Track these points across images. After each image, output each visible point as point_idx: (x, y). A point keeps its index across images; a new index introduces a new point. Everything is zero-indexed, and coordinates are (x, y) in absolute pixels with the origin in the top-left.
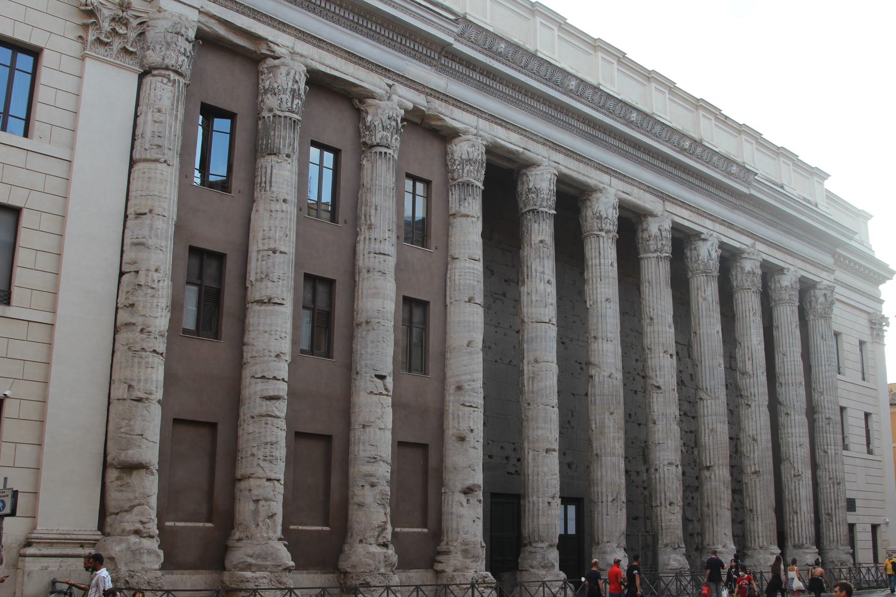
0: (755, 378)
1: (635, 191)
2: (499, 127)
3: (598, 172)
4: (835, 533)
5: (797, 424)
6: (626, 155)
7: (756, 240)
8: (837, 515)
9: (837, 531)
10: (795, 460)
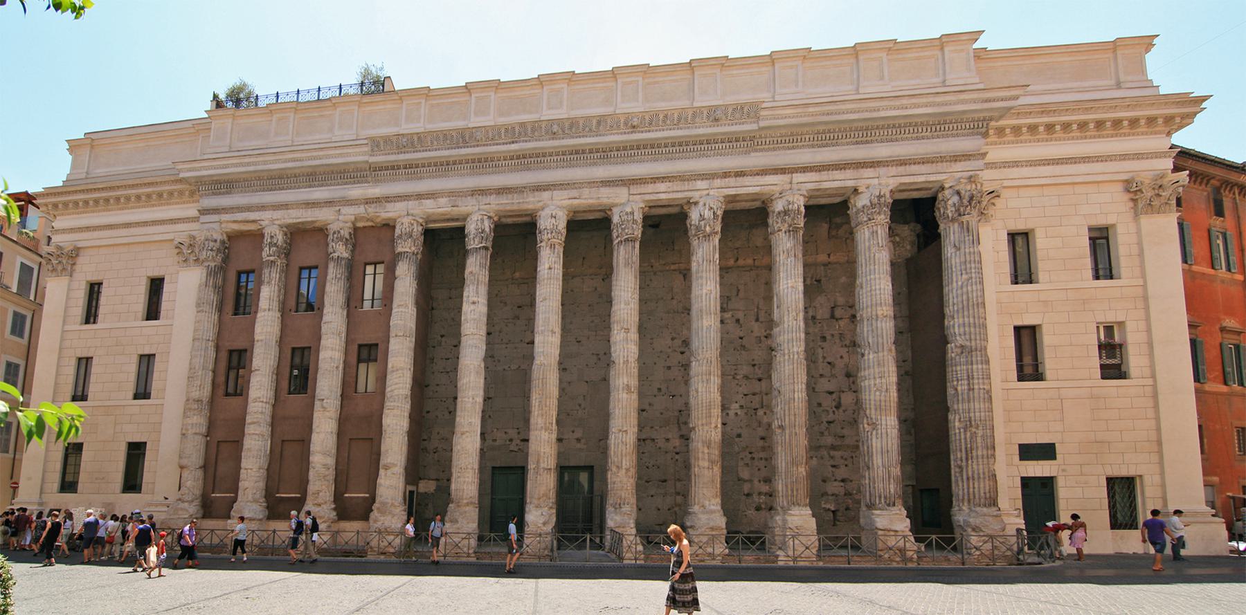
0: (781, 327)
1: (586, 192)
2: (428, 202)
3: (536, 193)
4: (966, 490)
5: (871, 365)
7: (793, 173)
8: (970, 467)
9: (968, 488)
10: (868, 406)
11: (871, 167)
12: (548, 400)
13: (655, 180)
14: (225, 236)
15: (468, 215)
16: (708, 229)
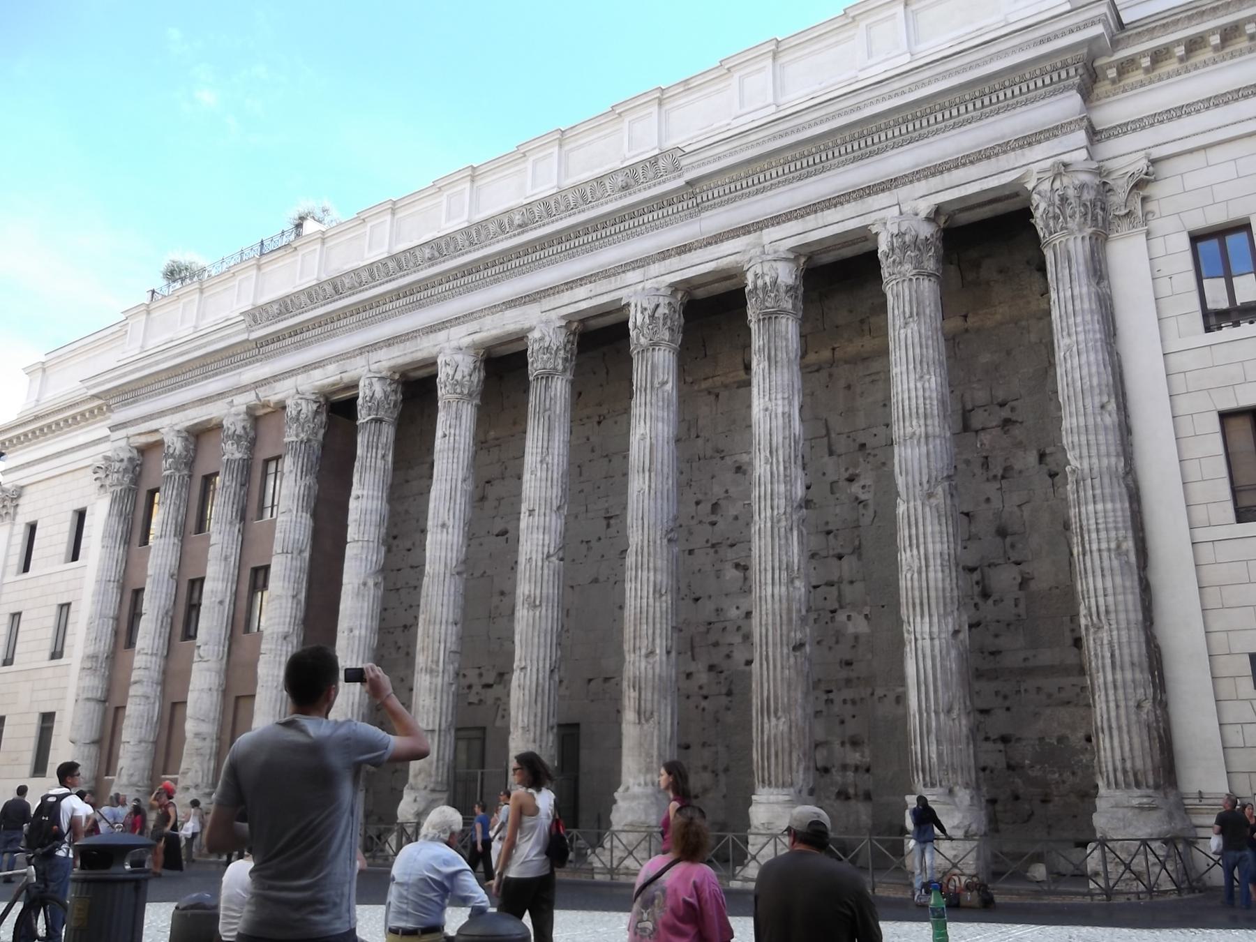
3: (432, 336)
6: (469, 289)
7: (762, 229)
11: (883, 190)
12: (431, 627)
13: (570, 285)
14: (135, 452)
15: (358, 381)
16: (642, 340)
